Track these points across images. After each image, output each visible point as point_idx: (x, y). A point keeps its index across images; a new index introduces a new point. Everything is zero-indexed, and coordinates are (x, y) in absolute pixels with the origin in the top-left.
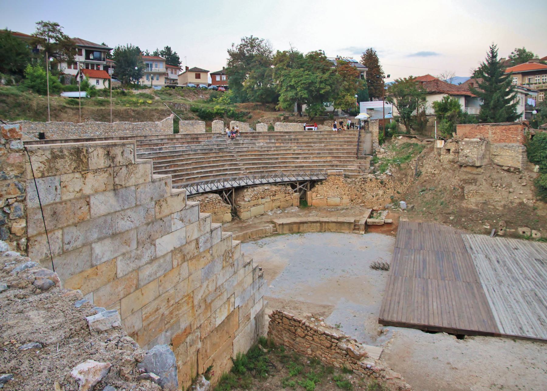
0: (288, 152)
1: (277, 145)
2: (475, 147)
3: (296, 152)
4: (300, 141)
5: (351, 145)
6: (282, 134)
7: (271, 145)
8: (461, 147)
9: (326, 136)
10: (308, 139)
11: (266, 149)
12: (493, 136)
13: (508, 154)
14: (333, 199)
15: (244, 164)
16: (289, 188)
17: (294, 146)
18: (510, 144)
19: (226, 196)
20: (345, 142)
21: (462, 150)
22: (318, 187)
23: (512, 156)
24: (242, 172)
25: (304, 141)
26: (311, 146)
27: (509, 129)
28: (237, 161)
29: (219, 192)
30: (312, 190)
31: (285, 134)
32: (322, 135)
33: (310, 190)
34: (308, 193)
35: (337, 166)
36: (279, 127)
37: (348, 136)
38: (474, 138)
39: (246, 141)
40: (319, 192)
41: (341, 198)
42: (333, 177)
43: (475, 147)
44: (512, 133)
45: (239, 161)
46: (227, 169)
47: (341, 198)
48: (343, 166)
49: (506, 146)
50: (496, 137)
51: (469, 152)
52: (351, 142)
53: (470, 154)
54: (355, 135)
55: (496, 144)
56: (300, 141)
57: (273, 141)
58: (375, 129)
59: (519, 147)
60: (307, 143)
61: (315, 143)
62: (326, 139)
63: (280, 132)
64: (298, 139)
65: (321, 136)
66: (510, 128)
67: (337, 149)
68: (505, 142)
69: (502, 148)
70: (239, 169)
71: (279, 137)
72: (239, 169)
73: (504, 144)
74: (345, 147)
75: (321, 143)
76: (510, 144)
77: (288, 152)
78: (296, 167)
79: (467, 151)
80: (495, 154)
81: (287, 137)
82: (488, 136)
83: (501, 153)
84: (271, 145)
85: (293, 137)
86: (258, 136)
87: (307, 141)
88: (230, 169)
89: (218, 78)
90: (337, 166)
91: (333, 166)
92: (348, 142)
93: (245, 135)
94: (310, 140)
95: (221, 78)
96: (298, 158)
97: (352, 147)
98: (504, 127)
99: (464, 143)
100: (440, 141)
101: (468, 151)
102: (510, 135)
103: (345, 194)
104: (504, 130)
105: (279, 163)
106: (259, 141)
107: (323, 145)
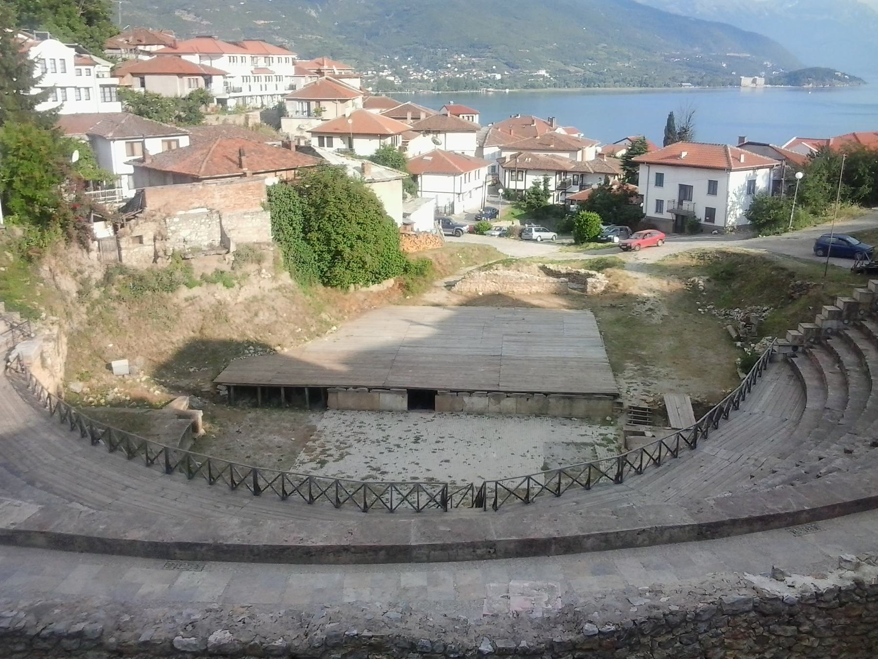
8: (172, 228)
12: (222, 200)
13: (250, 225)
18: (251, 210)
21: (174, 232)
27: (248, 188)
44: (253, 194)
50: (227, 203)
53: (193, 237)
68: (242, 207)
73: (242, 211)
82: (214, 201)
83: (240, 226)
101: (188, 231)
102: (251, 197)
104: (240, 189)
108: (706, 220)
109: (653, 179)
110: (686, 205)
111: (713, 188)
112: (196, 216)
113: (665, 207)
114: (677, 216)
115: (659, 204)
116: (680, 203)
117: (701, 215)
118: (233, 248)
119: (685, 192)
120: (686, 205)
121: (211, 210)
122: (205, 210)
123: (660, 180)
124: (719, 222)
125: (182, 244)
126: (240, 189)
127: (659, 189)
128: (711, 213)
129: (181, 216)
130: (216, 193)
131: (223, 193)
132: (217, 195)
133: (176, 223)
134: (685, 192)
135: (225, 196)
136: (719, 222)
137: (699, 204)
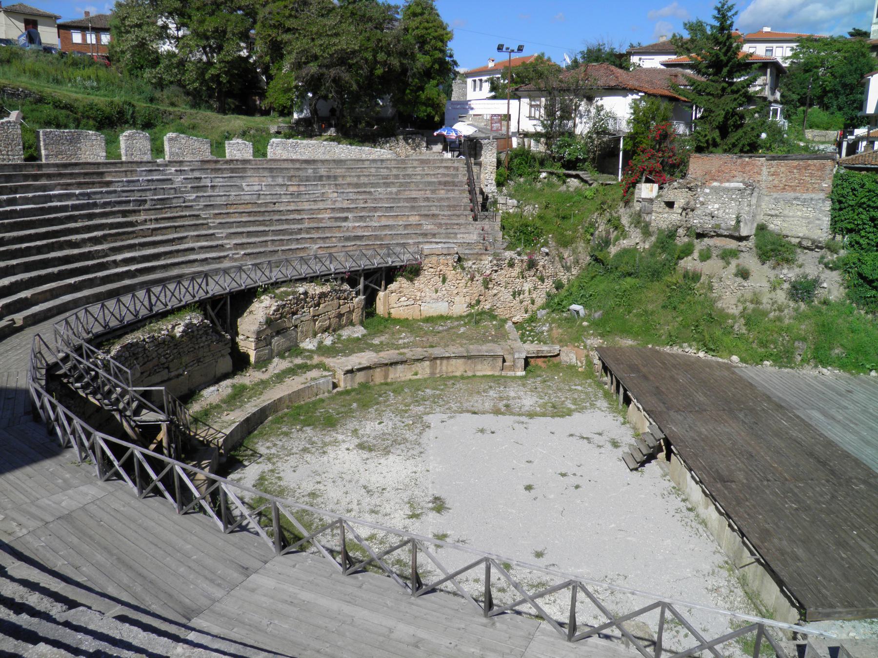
0: (321, 205)
1: (291, 189)
3: (338, 205)
4: (340, 181)
5: (453, 190)
6: (298, 166)
7: (278, 190)
8: (701, 199)
9: (395, 172)
10: (359, 176)
11: (269, 199)
12: (771, 178)
13: (799, 213)
14: (434, 305)
15: (230, 236)
16: (346, 286)
17: (330, 192)
18: (805, 196)
19: (213, 314)
20: (440, 183)
21: (702, 204)
22: (400, 283)
24: (230, 253)
25: (348, 180)
26: (370, 192)
28: (210, 228)
29: (201, 305)
30: (393, 286)
31: (304, 166)
32: (387, 168)
33: (386, 288)
34: (381, 294)
35: (434, 235)
36: (279, 149)
37: (442, 171)
38: (728, 181)
39: (218, 182)
40: (406, 291)
41: (451, 303)
42: (435, 258)
43: (733, 199)
44: (811, 175)
45: (215, 228)
46: (192, 250)
47: (451, 303)
48: (447, 236)
49: (796, 199)
50: (776, 182)
51: (718, 209)
52: (454, 184)
53: (720, 213)
54: (457, 169)
55: (775, 195)
56: (340, 181)
57: (280, 181)
58: (489, 157)
59: (824, 201)
60: (357, 185)
61: (373, 185)
62: (397, 176)
63: (292, 161)
64: (335, 178)
65: (384, 172)
67: (427, 199)
68: (795, 190)
69: (789, 202)
70: (221, 247)
71: (292, 173)
72: (221, 247)
73: (792, 195)
74: (442, 193)
75: (387, 185)
76: (805, 196)
77: (321, 205)
78: (348, 239)
79: (713, 207)
80: (773, 212)
81: (310, 171)
82: (759, 178)
83: (786, 212)
84: (278, 190)
85: (323, 172)
86: (244, 170)
87: (355, 180)
88: (201, 248)
89: (77, 37)
90: (434, 235)
91: (425, 235)
92: (445, 183)
93: (213, 166)
94: (364, 180)
95: (84, 38)
96: (346, 219)
97: (456, 194)
99: (707, 191)
100: (648, 185)
101: (717, 206)
102: (808, 179)
103: (457, 294)
104: (795, 167)
105: (308, 230)
106: (251, 181)
107: (394, 190)
112: (728, 190)
122: (741, 185)
126: (795, 167)
129: (711, 188)
130: (764, 169)
131: (772, 170)
132: (765, 170)
133: (707, 194)
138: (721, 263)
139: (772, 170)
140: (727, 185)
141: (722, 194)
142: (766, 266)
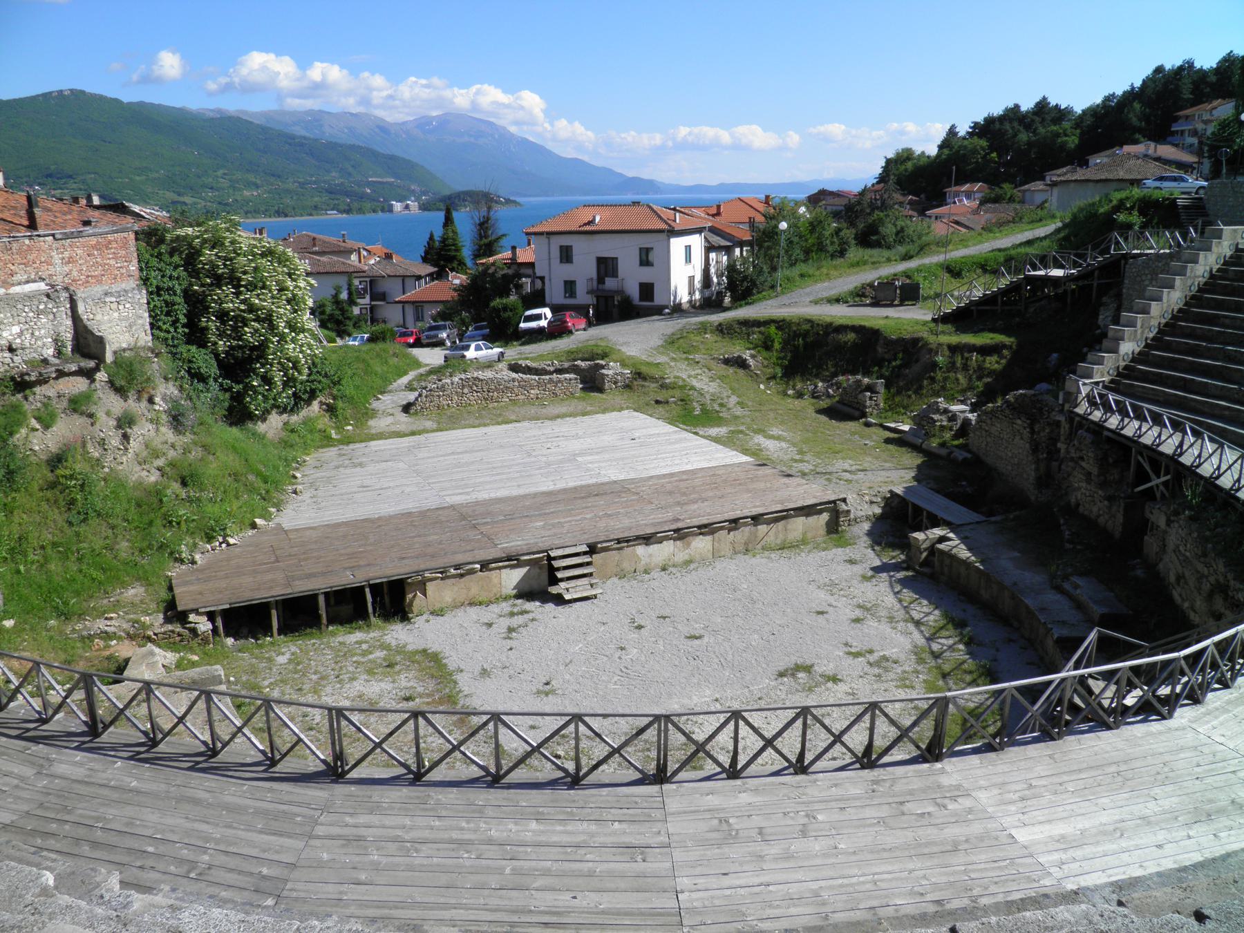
2: (43, 312)
13: (116, 315)
23: (127, 318)
43: (39, 313)
51: (21, 334)
53: (27, 340)
66: (110, 242)
68: (100, 282)
82: (52, 270)
83: (99, 317)
98: (93, 241)
101: (16, 329)
102: (112, 262)
104: (93, 247)
108: (641, 299)
109: (556, 253)
110: (610, 283)
111: (645, 259)
112: (30, 297)
113: (581, 289)
114: (598, 297)
115: (570, 286)
116: (601, 280)
117: (634, 292)
118: (109, 358)
119: (607, 266)
120: (610, 283)
121: (53, 286)
122: (42, 286)
123: (566, 255)
124: (658, 300)
125: (7, 354)
127: (566, 266)
128: (647, 290)
131: (66, 254)
132: (57, 259)
134: (607, 266)
135: (70, 261)
136: (658, 300)
137: (630, 277)
138: (79, 421)
139: (66, 254)
140: (17, 289)
141: (20, 306)
142: (130, 401)
